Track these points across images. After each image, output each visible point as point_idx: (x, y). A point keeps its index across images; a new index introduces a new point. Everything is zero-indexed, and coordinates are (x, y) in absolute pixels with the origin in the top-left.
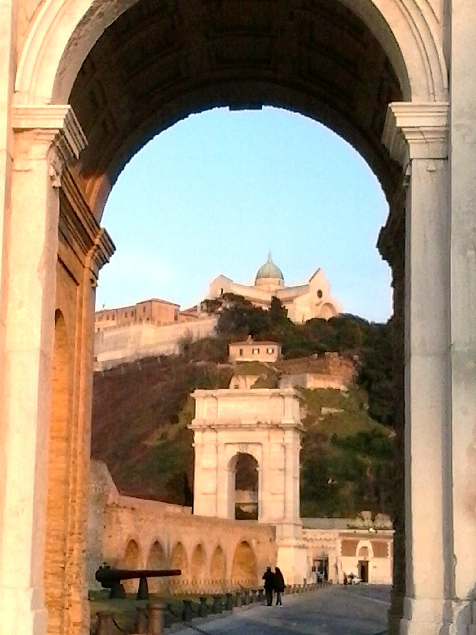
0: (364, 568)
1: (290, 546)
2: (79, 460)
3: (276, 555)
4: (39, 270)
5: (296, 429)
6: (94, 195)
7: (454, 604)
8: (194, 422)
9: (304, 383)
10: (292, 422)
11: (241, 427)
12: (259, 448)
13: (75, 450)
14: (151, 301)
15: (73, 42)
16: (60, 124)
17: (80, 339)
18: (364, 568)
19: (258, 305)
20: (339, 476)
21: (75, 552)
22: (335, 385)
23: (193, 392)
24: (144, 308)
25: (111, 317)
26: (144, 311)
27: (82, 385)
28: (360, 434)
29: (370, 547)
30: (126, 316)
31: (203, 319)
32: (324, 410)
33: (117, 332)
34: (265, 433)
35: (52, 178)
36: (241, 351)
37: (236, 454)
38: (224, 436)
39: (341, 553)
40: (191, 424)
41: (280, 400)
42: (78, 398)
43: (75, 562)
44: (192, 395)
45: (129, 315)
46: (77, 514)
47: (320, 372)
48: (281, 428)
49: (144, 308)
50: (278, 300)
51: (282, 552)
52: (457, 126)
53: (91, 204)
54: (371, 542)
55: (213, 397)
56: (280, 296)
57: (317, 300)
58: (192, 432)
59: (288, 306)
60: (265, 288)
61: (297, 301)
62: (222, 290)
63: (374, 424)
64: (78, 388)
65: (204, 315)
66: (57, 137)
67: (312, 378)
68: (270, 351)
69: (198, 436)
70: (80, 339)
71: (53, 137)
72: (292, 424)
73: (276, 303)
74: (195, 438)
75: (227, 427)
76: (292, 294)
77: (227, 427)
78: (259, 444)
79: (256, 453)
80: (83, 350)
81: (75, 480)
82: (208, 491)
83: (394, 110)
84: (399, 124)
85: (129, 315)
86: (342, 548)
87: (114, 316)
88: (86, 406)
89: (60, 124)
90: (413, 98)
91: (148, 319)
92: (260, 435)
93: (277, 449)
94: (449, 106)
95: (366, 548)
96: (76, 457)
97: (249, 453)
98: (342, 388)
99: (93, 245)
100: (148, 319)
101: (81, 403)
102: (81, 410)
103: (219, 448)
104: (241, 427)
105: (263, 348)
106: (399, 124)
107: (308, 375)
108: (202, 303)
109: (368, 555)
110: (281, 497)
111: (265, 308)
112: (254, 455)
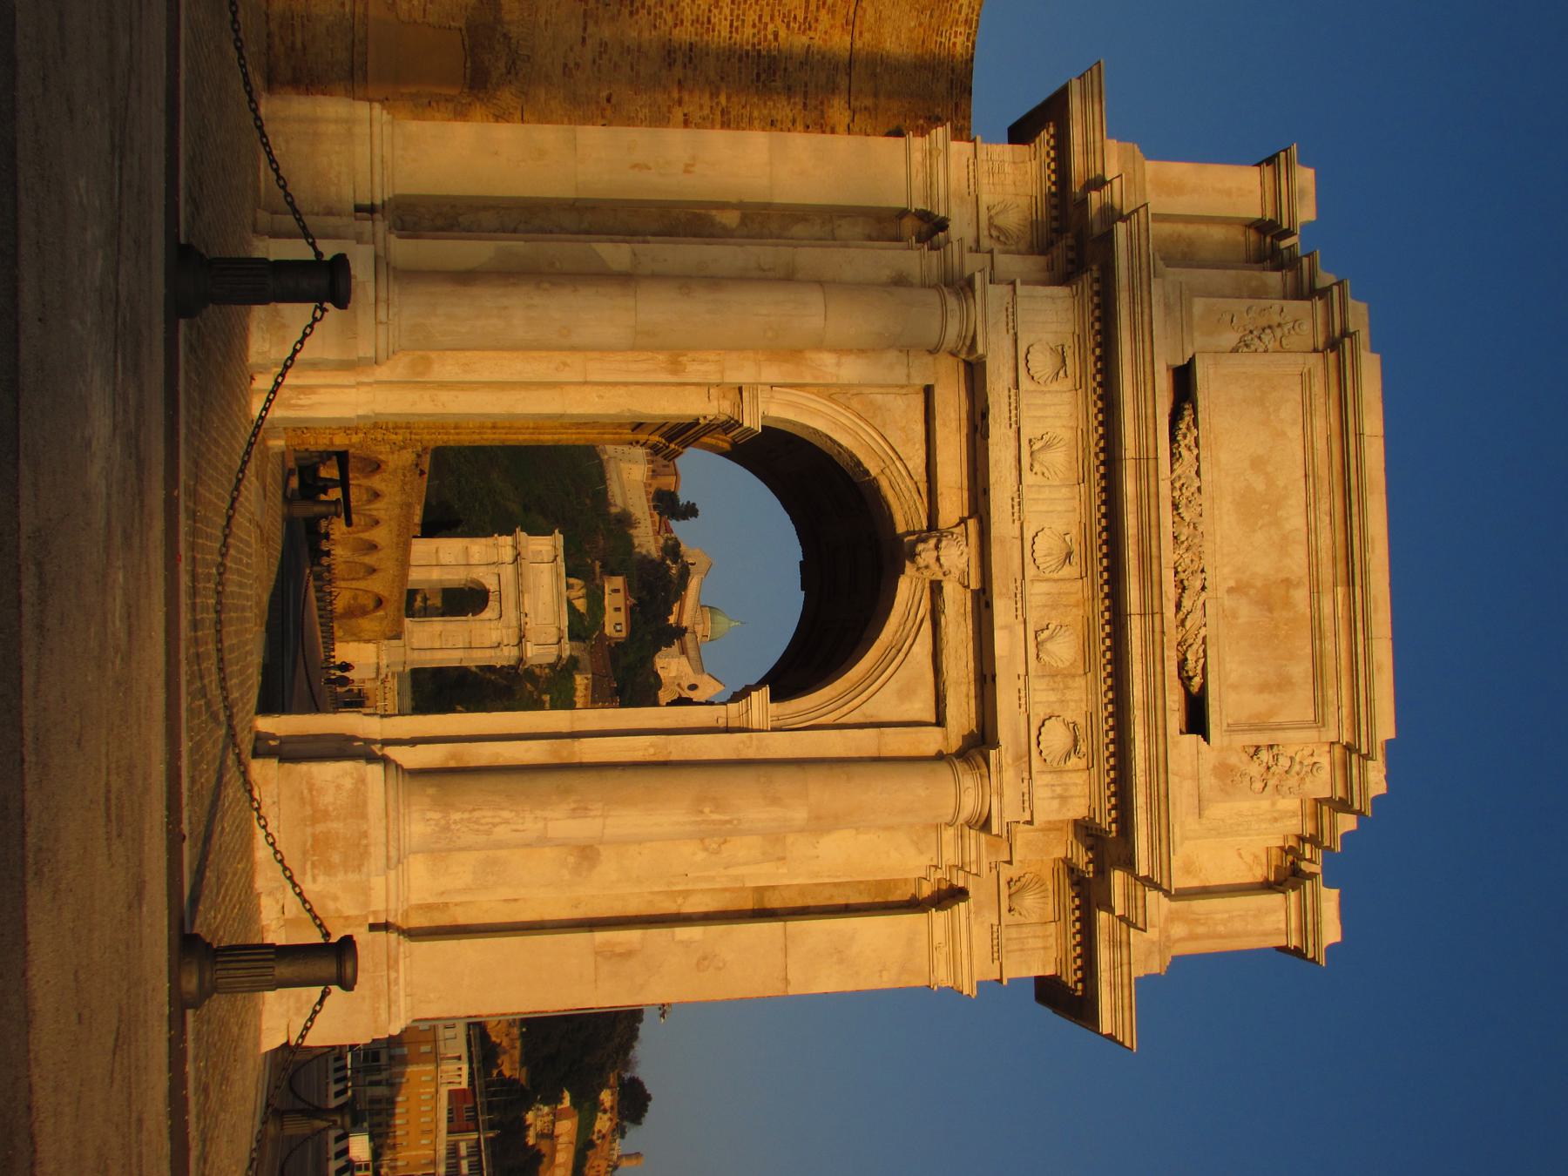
2: (476, 437)
3: (369, 641)
4: (629, 410)
5: (521, 660)
6: (713, 441)
7: (379, 746)
8: (523, 535)
9: (580, 671)
10: (529, 655)
11: (520, 593)
12: (496, 615)
13: (485, 433)
14: (676, 474)
15: (816, 431)
16: (746, 424)
17: (584, 433)
19: (675, 608)
21: (394, 436)
23: (560, 532)
27: (541, 437)
31: (656, 541)
34: (514, 623)
35: (705, 418)
36: (616, 591)
37: (488, 587)
38: (508, 572)
40: (522, 531)
41: (555, 640)
42: (533, 434)
43: (386, 437)
44: (557, 531)
46: (428, 437)
47: (594, 691)
48: (520, 642)
50: (684, 635)
51: (371, 647)
52: (751, 737)
53: (705, 439)
55: (556, 556)
56: (688, 637)
57: (685, 684)
58: (510, 532)
59: (675, 648)
60: (699, 619)
61: (684, 659)
62: (692, 564)
64: (540, 434)
65: (662, 541)
66: (737, 422)
68: (618, 628)
69: (508, 540)
70: (584, 433)
71: (736, 418)
73: (679, 632)
74: (504, 537)
75: (519, 575)
76: (692, 653)
77: (519, 575)
79: (488, 613)
80: (574, 436)
81: (458, 434)
82: (441, 555)
83: (764, 689)
84: (753, 693)
88: (525, 440)
89: (746, 424)
90: (774, 705)
92: (511, 614)
93: (495, 637)
94: (767, 731)
96: (479, 433)
97: (490, 603)
99: (670, 442)
100: (653, 471)
101: (527, 437)
102: (521, 437)
103: (493, 566)
104: (520, 593)
105: (621, 617)
106: (753, 693)
107: (590, 676)
110: (437, 645)
111: (672, 619)
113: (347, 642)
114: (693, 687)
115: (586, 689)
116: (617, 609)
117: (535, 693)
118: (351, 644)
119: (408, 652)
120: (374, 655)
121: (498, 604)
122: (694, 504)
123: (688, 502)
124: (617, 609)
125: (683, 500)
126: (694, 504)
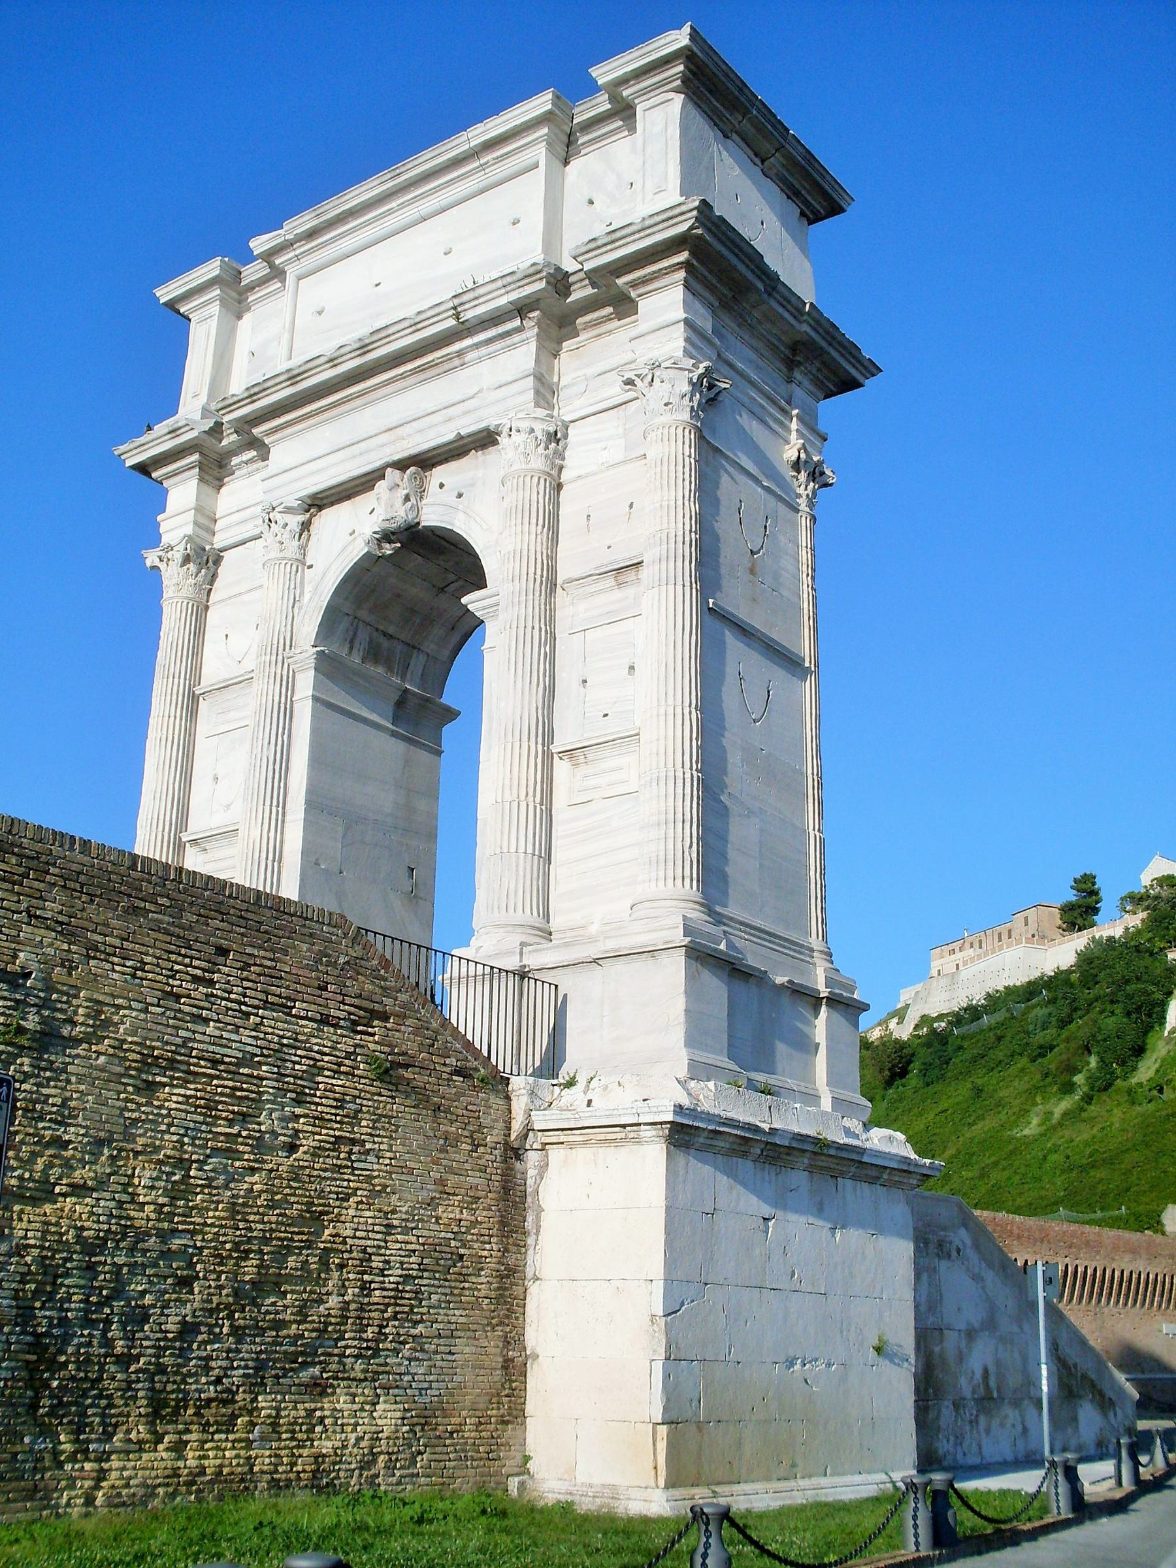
24: (1026, 919)
25: (976, 945)
26: (1026, 924)
30: (1000, 940)
33: (981, 965)
45: (1005, 937)
49: (1026, 919)
78: (486, 439)
85: (1005, 937)
87: (980, 941)
91: (1033, 936)
97: (430, 518)
108: (1122, 899)
112: (461, 526)
118: (532, 1338)
121: (439, 474)
122: (1075, 881)
123: (1072, 888)
125: (1071, 896)
126: (1075, 881)
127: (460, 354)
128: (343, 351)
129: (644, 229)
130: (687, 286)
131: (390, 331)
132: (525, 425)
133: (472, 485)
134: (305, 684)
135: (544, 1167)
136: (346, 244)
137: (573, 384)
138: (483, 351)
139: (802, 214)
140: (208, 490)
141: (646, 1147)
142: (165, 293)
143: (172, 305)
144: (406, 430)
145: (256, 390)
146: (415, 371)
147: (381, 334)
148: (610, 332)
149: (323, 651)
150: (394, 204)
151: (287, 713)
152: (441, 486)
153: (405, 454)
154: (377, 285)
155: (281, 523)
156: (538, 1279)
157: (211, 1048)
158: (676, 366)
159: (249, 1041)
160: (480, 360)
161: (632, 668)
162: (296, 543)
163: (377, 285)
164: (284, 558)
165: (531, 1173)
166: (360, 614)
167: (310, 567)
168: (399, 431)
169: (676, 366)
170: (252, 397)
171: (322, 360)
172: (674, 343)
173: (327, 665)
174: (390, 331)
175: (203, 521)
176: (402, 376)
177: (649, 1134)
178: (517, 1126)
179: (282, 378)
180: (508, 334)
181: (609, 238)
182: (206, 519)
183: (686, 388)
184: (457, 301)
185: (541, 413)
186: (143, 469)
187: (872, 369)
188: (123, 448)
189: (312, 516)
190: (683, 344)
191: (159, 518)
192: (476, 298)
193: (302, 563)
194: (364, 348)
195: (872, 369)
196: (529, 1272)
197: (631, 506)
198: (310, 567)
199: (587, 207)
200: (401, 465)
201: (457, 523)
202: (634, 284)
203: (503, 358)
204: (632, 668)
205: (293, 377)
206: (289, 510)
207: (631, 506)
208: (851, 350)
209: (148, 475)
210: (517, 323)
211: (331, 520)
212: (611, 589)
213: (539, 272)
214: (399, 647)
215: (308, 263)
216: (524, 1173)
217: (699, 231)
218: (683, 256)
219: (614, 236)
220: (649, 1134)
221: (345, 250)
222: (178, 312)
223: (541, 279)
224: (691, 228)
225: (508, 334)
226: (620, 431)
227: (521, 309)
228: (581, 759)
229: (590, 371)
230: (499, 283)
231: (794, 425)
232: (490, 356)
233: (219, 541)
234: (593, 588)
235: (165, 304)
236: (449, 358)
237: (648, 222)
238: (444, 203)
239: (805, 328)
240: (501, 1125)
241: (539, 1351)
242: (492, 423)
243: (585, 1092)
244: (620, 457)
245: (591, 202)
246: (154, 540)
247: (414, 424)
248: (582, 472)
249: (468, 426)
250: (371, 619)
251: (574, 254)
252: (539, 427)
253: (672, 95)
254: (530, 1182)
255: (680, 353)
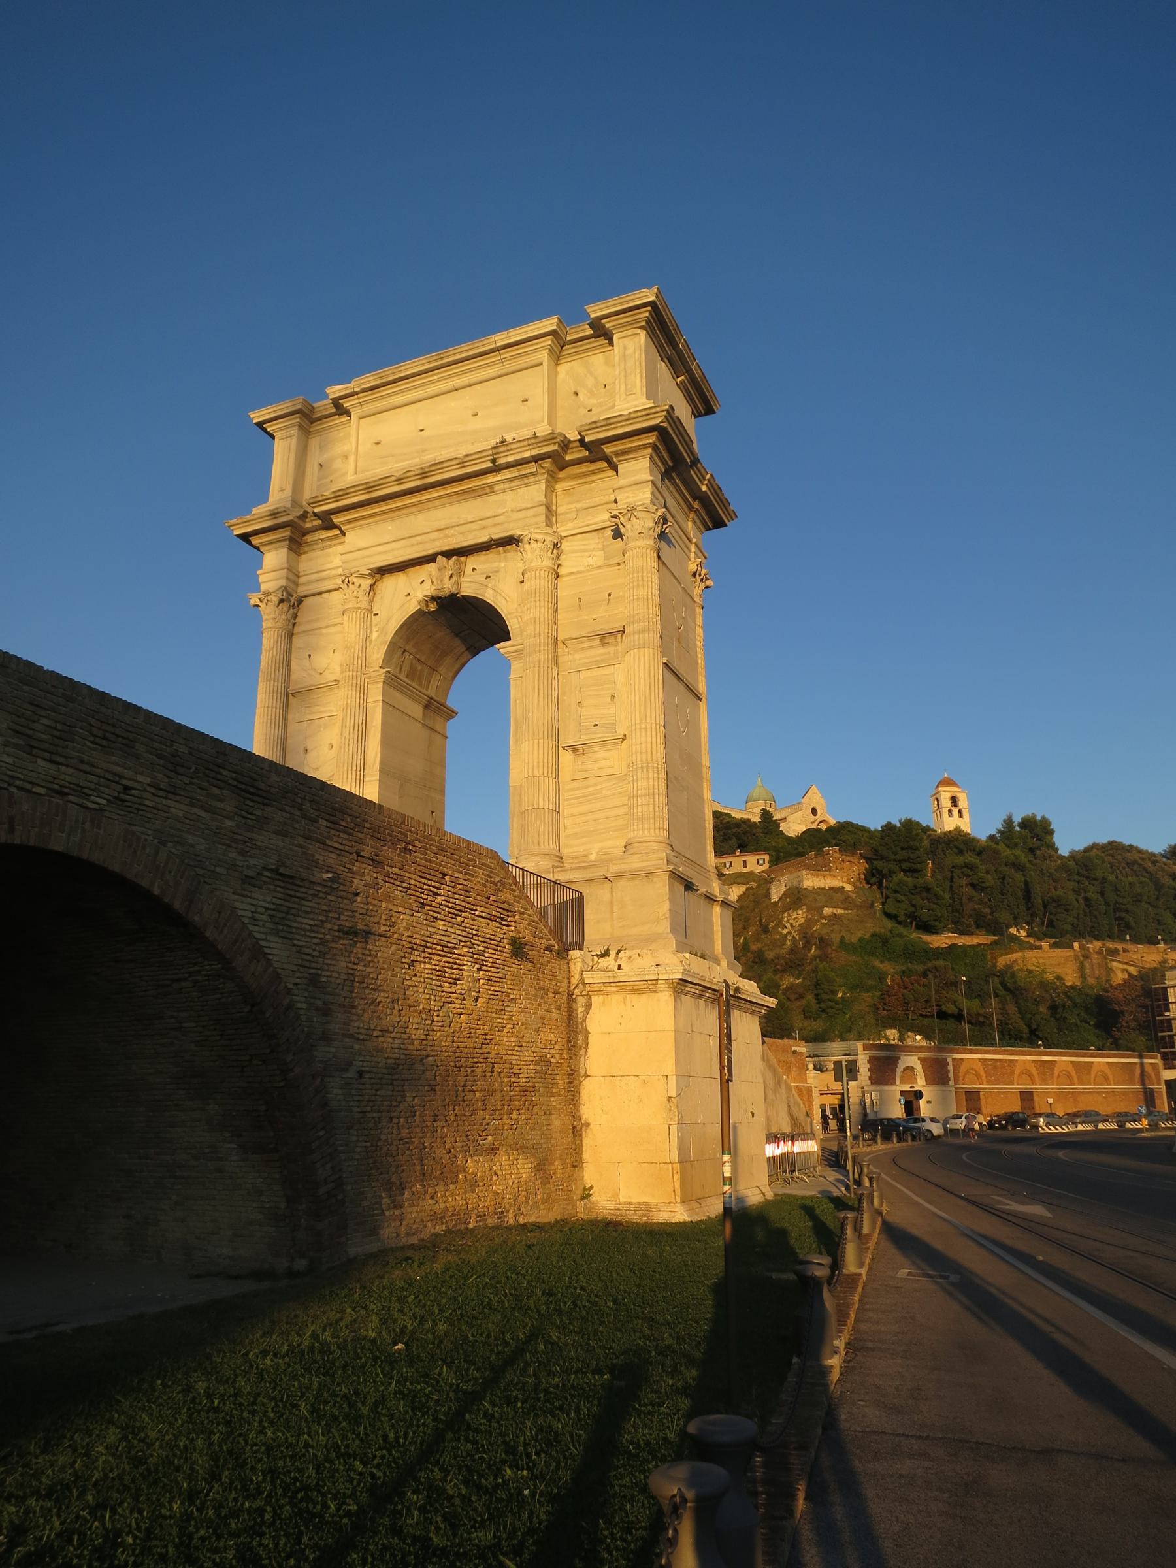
0: (911, 1101)
1: (650, 987)
9: (800, 882)
18: (911, 1101)
20: (853, 988)
22: (836, 883)
28: (874, 935)
29: (918, 1068)
32: (827, 911)
34: (535, 491)
39: (870, 1078)
54: (919, 1059)
57: (812, 818)
63: (889, 924)
67: (809, 876)
68: (761, 862)
72: (647, 413)
73: (765, 814)
76: (784, 814)
78: (510, 541)
86: (869, 1070)
95: (910, 1069)
97: (468, 589)
98: (848, 888)
105: (751, 859)
109: (916, 1082)
112: (489, 597)
113: (577, 1131)
114: (814, 811)
115: (817, 876)
116: (744, 862)
117: (823, 921)
118: (586, 1113)
119: (636, 863)
120: (641, 1002)
121: (472, 562)
124: (744, 862)
127: (491, 485)
128: (408, 474)
129: (630, 418)
130: (651, 458)
131: (445, 465)
132: (540, 537)
133: (497, 572)
134: (376, 693)
135: (588, 1007)
136: (398, 400)
137: (567, 513)
138: (508, 485)
139: (693, 413)
140: (293, 555)
141: (660, 994)
142: (257, 416)
143: (260, 425)
144: (452, 531)
145: (340, 493)
146: (457, 493)
147: (437, 465)
148: (592, 482)
149: (389, 672)
150: (436, 377)
151: (364, 710)
152: (474, 569)
153: (451, 547)
154: (422, 430)
155: (357, 584)
156: (588, 1076)
157: (443, 938)
158: (646, 509)
159: (459, 932)
160: (505, 491)
161: (613, 697)
162: (366, 598)
163: (422, 430)
164: (359, 608)
165: (581, 1010)
166: (407, 648)
167: (376, 614)
168: (447, 532)
169: (646, 509)
170: (337, 497)
171: (393, 478)
172: (645, 495)
173: (391, 682)
174: (445, 465)
175: (292, 576)
176: (447, 495)
177: (663, 986)
178: (574, 981)
179: (361, 488)
180: (526, 476)
181: (605, 423)
182: (293, 575)
183: (652, 524)
184: (494, 451)
185: (549, 530)
186: (245, 537)
187: (733, 516)
188: (232, 522)
189: (377, 581)
190: (649, 495)
191: (258, 572)
192: (508, 451)
193: (370, 612)
194: (424, 474)
195: (733, 516)
196: (582, 1073)
197: (609, 595)
198: (376, 614)
199: (574, 397)
200: (448, 554)
201: (487, 595)
202: (617, 454)
203: (521, 491)
204: (613, 697)
205: (369, 487)
206: (362, 576)
207: (609, 595)
208: (725, 503)
209: (249, 543)
210: (532, 468)
211: (393, 585)
212: (597, 646)
213: (554, 438)
214: (427, 670)
215: (367, 409)
216: (577, 1010)
217: (665, 425)
218: (652, 438)
219: (609, 422)
220: (663, 986)
221: (397, 404)
222: (265, 430)
223: (555, 443)
224: (661, 422)
225: (526, 476)
226: (600, 546)
227: (536, 459)
228: (581, 751)
229: (579, 505)
230: (526, 443)
231: (693, 549)
232: (513, 489)
233: (302, 591)
234: (585, 645)
235: (256, 424)
236: (482, 487)
237: (632, 415)
238: (472, 381)
239: (704, 488)
240: (566, 980)
241: (590, 1121)
242: (516, 532)
243: (616, 960)
244: (601, 563)
245: (577, 394)
246: (256, 588)
247: (457, 528)
248: (575, 570)
249: (498, 534)
250: (413, 651)
251: (580, 429)
252: (548, 539)
253: (639, 331)
254: (580, 1015)
255: (648, 501)
